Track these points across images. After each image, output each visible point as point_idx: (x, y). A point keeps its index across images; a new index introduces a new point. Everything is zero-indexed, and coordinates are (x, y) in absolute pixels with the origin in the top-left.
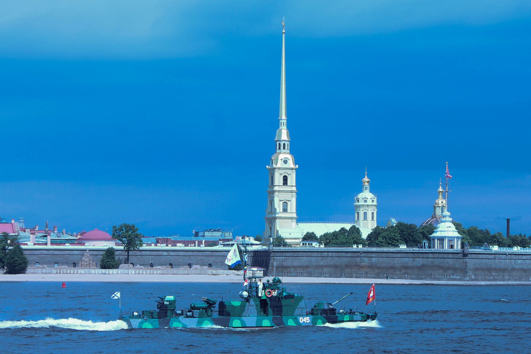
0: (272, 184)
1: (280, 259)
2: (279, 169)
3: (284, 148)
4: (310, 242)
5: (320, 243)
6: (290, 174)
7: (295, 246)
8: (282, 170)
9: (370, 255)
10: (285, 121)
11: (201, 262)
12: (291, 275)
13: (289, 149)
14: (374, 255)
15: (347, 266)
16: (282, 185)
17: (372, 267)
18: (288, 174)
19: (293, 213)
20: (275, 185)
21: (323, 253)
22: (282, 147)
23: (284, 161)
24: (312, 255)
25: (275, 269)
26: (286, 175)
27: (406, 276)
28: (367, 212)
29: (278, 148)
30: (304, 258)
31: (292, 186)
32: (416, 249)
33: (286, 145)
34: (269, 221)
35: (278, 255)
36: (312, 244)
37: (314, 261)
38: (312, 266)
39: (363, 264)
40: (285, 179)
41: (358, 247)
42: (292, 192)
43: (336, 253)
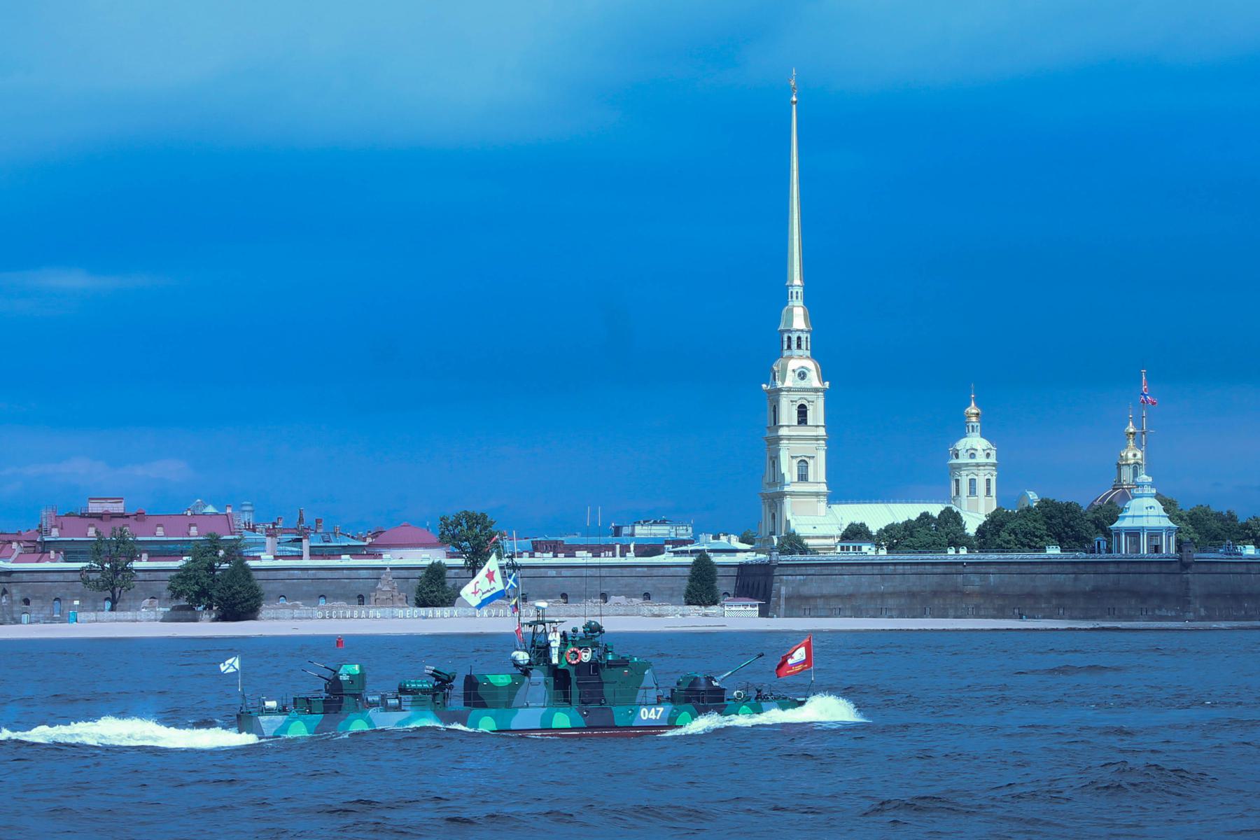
0: (775, 423)
1: (793, 581)
2: (789, 390)
3: (799, 346)
4: (857, 545)
5: (879, 546)
6: (813, 402)
7: (825, 553)
8: (795, 393)
9: (983, 569)
10: (800, 290)
11: (627, 589)
12: (819, 614)
13: (809, 348)
14: (992, 569)
15: (935, 594)
16: (796, 424)
17: (987, 594)
18: (809, 402)
19: (820, 483)
20: (781, 424)
21: (885, 567)
22: (794, 345)
23: (799, 375)
24: (862, 572)
25: (782, 602)
26: (803, 403)
27: (1061, 612)
28: (975, 480)
29: (785, 347)
30: (844, 578)
31: (817, 426)
32: (1081, 556)
33: (803, 339)
34: (770, 500)
35: (789, 572)
36: (860, 548)
37: (865, 582)
38: (863, 594)
39: (969, 588)
40: (802, 411)
41: (957, 552)
42: (817, 439)
43: (913, 567)
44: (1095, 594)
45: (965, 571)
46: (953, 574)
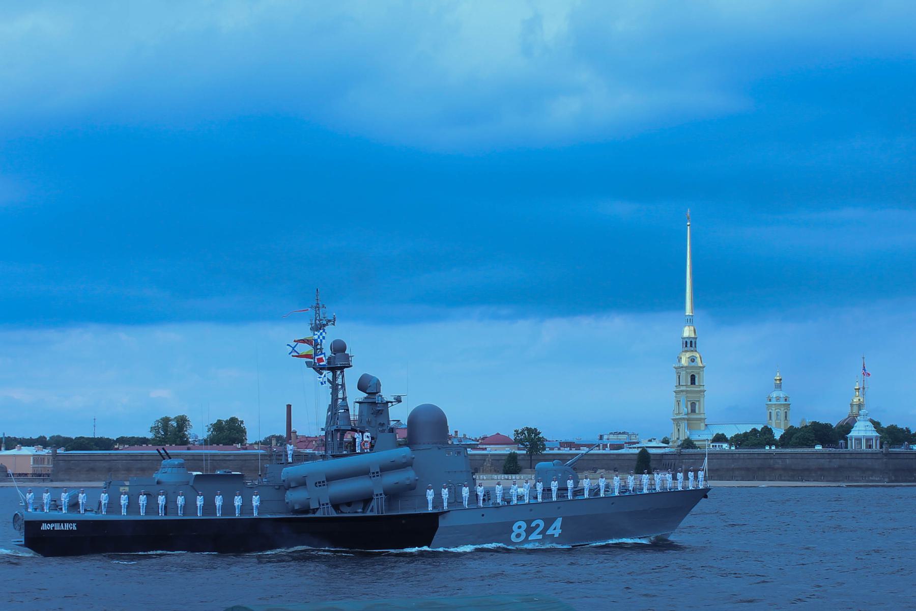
3: (691, 346)
4: (720, 444)
5: (731, 445)
6: (698, 373)
15: (759, 469)
17: (785, 469)
21: (734, 455)
22: (689, 345)
23: (691, 360)
27: (822, 478)
29: (684, 346)
33: (693, 342)
35: (687, 458)
36: (722, 446)
39: (777, 466)
41: (770, 448)
44: (840, 469)
45: (774, 457)
46: (768, 459)
